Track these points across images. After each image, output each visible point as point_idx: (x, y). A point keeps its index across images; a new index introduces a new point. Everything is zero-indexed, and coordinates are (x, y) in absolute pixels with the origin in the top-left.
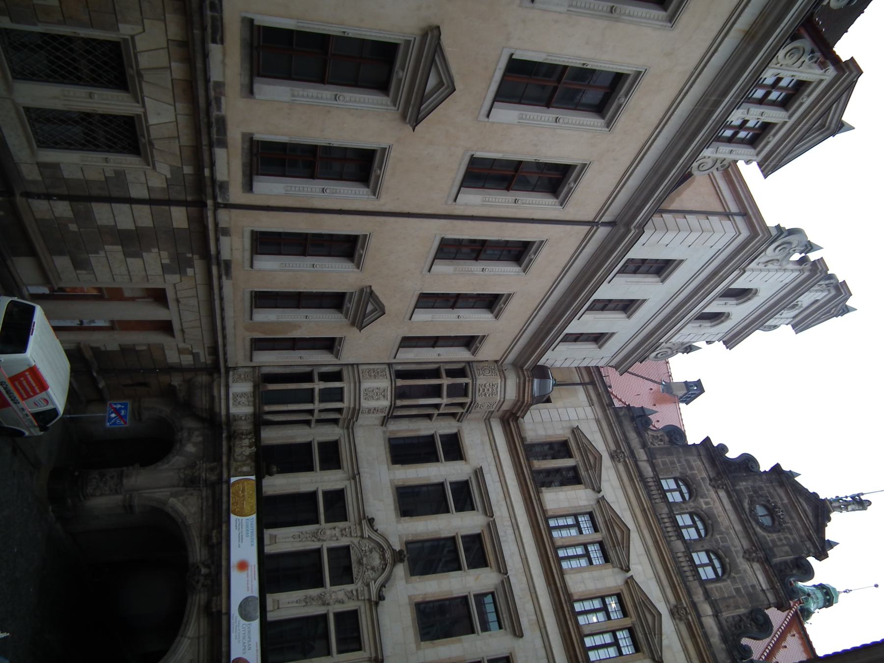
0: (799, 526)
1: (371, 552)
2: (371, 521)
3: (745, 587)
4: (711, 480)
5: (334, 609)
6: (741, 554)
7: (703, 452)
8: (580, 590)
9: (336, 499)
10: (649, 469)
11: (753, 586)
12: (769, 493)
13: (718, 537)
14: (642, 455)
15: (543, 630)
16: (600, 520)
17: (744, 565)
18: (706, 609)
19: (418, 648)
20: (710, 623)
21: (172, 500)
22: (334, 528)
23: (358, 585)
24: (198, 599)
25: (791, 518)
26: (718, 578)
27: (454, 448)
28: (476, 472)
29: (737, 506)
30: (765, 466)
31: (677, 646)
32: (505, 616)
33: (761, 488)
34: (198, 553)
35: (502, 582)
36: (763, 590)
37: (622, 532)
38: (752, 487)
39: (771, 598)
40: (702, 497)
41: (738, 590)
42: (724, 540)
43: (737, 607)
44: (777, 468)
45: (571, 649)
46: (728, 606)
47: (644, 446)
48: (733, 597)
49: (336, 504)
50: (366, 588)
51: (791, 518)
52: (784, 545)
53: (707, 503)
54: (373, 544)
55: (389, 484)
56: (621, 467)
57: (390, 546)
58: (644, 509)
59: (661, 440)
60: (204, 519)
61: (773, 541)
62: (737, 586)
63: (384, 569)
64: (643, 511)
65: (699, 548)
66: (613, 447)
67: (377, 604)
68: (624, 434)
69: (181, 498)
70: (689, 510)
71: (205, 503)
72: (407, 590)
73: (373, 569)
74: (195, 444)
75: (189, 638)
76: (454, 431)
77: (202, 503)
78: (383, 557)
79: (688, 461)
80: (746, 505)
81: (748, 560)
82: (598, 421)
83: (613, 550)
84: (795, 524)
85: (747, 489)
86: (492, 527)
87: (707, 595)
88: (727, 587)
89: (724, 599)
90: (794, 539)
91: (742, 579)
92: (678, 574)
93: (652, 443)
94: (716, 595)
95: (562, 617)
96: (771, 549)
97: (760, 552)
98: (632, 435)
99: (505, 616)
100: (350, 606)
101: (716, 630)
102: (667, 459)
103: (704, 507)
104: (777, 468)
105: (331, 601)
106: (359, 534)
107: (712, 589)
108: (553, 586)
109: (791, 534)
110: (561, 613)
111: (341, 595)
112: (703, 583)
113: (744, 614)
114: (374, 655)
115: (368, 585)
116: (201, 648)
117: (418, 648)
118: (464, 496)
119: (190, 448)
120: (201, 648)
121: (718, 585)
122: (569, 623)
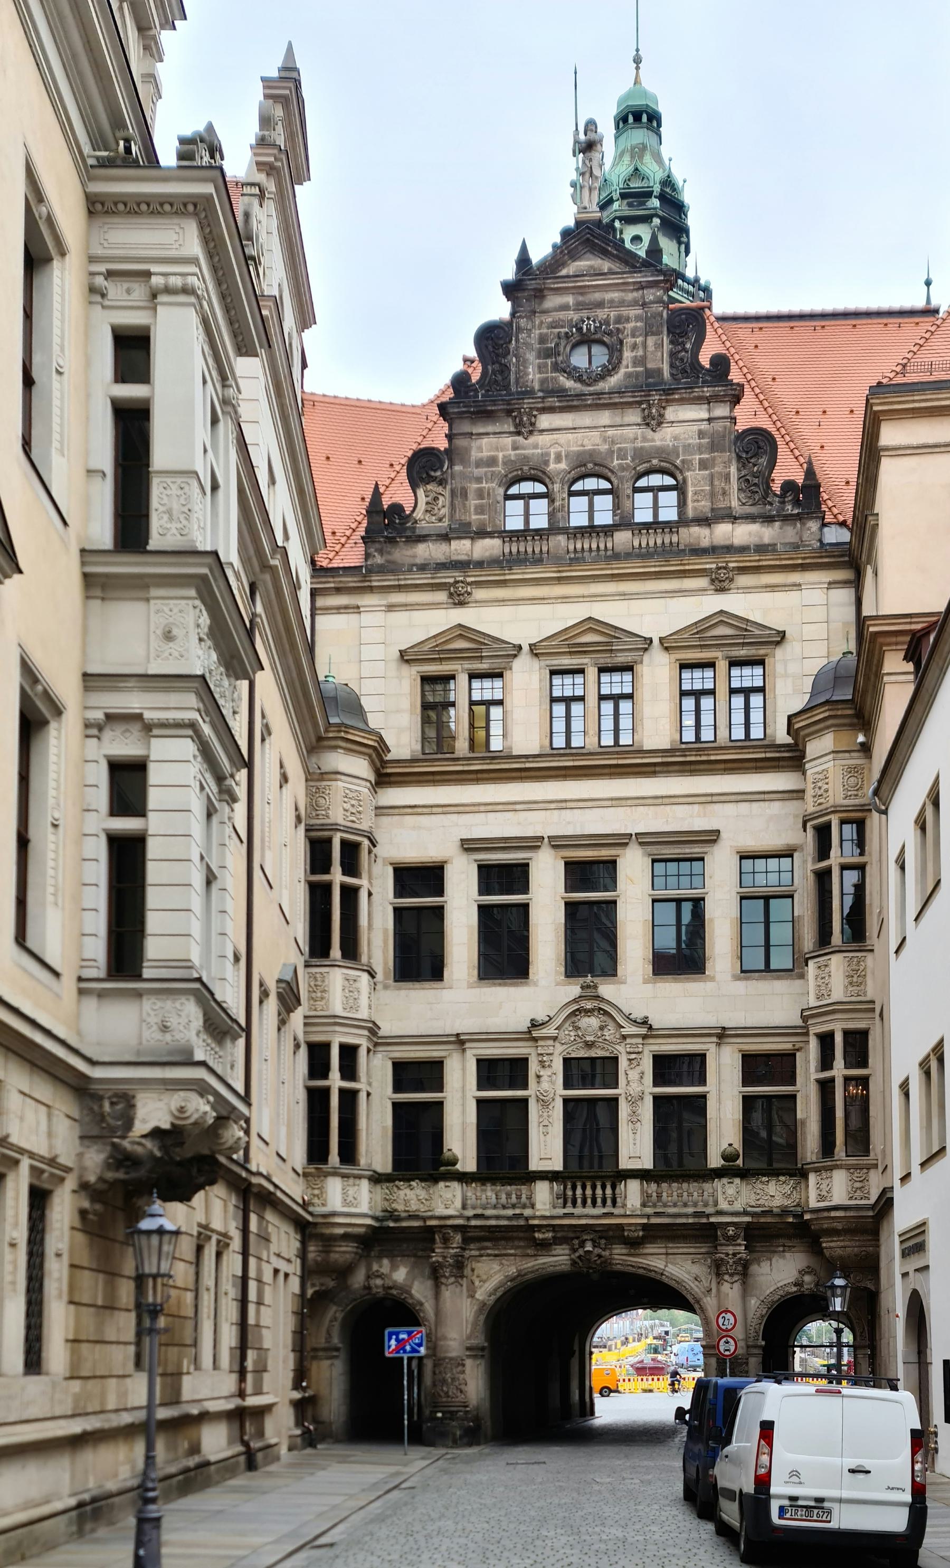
0: (615, 295)
1: (577, 1028)
2: (534, 1024)
3: (700, 449)
4: (519, 433)
5: (649, 1088)
6: (649, 433)
7: (466, 427)
8: (668, 727)
9: (492, 1071)
10: (488, 542)
11: (701, 434)
12: (553, 325)
13: (616, 462)
14: (461, 548)
15: (715, 799)
16: (567, 662)
17: (664, 437)
18: (723, 532)
19: (712, 979)
20: (743, 533)
21: (480, 1295)
22: (539, 1077)
23: (621, 1051)
24: (619, 1256)
25: (600, 305)
26: (680, 488)
27: (420, 879)
28: (467, 850)
29: (569, 403)
30: (501, 310)
31: (767, 598)
32: (687, 851)
33: (542, 339)
34: (559, 1259)
35: (641, 844)
36: (709, 420)
37: (591, 630)
38: (539, 357)
39: (721, 410)
40: (547, 463)
41: (703, 465)
42: (622, 454)
43: (727, 477)
44: (510, 290)
45: (747, 765)
46: (724, 493)
47: (445, 537)
48: (712, 477)
49: (501, 1072)
50: (628, 1041)
51: (600, 305)
52: (645, 345)
53: (558, 458)
54: (567, 1025)
55: (474, 990)
56: (480, 594)
57: (575, 1001)
58: (559, 579)
59: (436, 499)
60: (512, 1251)
61: (637, 362)
62: (696, 463)
63: (606, 1013)
64: (560, 580)
65: (628, 504)
66: (442, 596)
67: (650, 1028)
68: (423, 568)
69: (477, 1283)
70: (565, 495)
71: (489, 1251)
72: (634, 988)
73: (601, 1028)
74: (394, 1267)
75: (666, 1266)
76: (390, 871)
77: (489, 1255)
78: (589, 1012)
79: (479, 464)
80: (569, 384)
81: (660, 424)
82: (391, 608)
83: (614, 653)
84: (612, 304)
85: (541, 369)
86: (557, 843)
87: (705, 521)
88: (695, 479)
89: (713, 494)
90: (638, 318)
91: (687, 448)
92: (665, 555)
93: (440, 520)
94: (705, 505)
95: (702, 767)
96: (649, 373)
97: (650, 396)
98: (425, 551)
99: (688, 850)
100: (647, 1065)
101: (755, 527)
102: (473, 502)
103: (563, 466)
104: (510, 290)
105: (639, 1089)
106: (551, 1042)
107: (695, 509)
108: (657, 769)
109: (628, 320)
110: (697, 767)
111: (634, 1075)
112: (683, 521)
113: (739, 470)
114: (715, 1039)
115: (624, 1037)
116: (681, 1251)
117: (712, 979)
118: (504, 875)
119: (400, 1275)
120: (681, 1251)
121: (690, 494)
122: (713, 758)
